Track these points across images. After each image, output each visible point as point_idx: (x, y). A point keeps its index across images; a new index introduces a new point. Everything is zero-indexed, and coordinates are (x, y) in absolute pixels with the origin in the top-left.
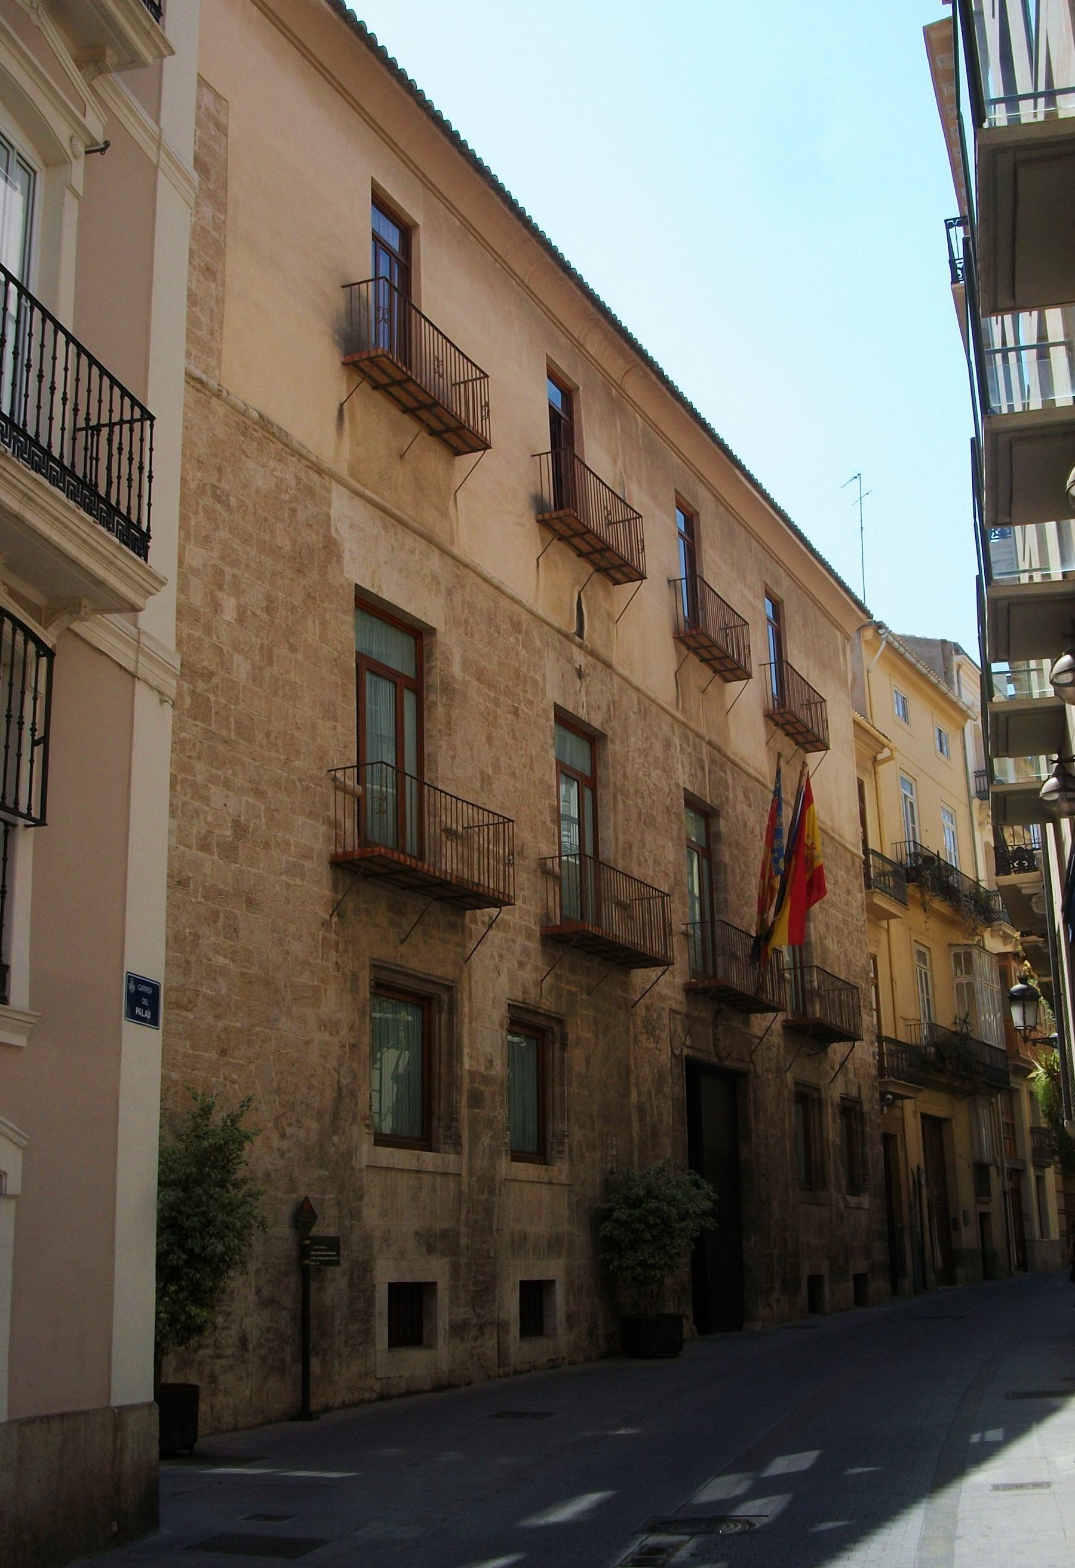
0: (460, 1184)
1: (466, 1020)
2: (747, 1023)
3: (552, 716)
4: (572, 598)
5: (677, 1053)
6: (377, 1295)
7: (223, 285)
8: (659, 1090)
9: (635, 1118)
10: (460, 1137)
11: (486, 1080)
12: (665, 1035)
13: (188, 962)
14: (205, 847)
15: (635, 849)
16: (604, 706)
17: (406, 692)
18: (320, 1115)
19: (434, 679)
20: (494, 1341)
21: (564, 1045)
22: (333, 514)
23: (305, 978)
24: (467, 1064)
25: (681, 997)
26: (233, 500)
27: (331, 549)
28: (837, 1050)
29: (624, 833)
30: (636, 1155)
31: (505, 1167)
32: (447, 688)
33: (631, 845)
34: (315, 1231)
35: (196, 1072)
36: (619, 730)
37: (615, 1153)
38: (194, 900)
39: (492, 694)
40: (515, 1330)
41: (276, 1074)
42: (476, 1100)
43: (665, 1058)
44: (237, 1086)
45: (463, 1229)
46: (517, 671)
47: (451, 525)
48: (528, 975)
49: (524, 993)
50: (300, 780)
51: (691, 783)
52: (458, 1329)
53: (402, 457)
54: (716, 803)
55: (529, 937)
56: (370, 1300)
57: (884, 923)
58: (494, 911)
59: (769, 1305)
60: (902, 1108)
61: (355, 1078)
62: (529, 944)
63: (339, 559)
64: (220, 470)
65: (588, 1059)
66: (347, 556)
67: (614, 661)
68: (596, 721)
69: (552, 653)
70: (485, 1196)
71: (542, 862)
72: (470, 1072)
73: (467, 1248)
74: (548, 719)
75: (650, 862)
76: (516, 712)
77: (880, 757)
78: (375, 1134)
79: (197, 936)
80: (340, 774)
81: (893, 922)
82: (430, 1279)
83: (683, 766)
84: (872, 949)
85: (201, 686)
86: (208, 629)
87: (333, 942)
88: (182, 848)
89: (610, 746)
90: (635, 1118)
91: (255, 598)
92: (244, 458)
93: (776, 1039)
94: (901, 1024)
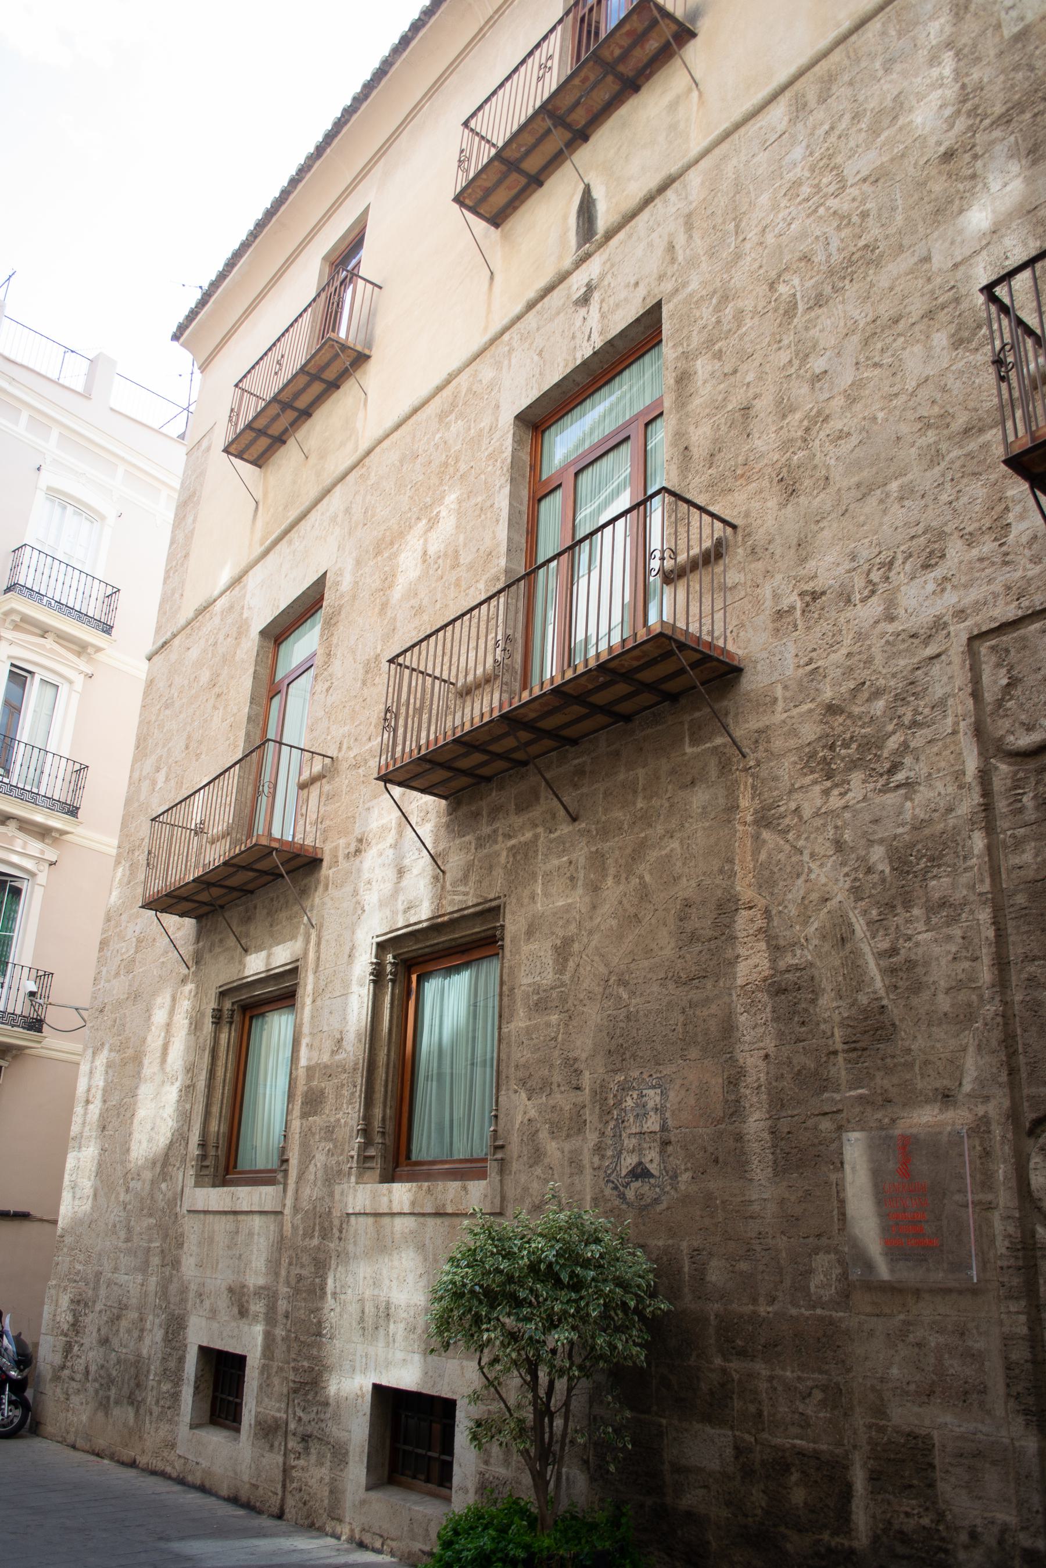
0: (281, 1225)
56: (181, 1360)
70: (316, 1242)
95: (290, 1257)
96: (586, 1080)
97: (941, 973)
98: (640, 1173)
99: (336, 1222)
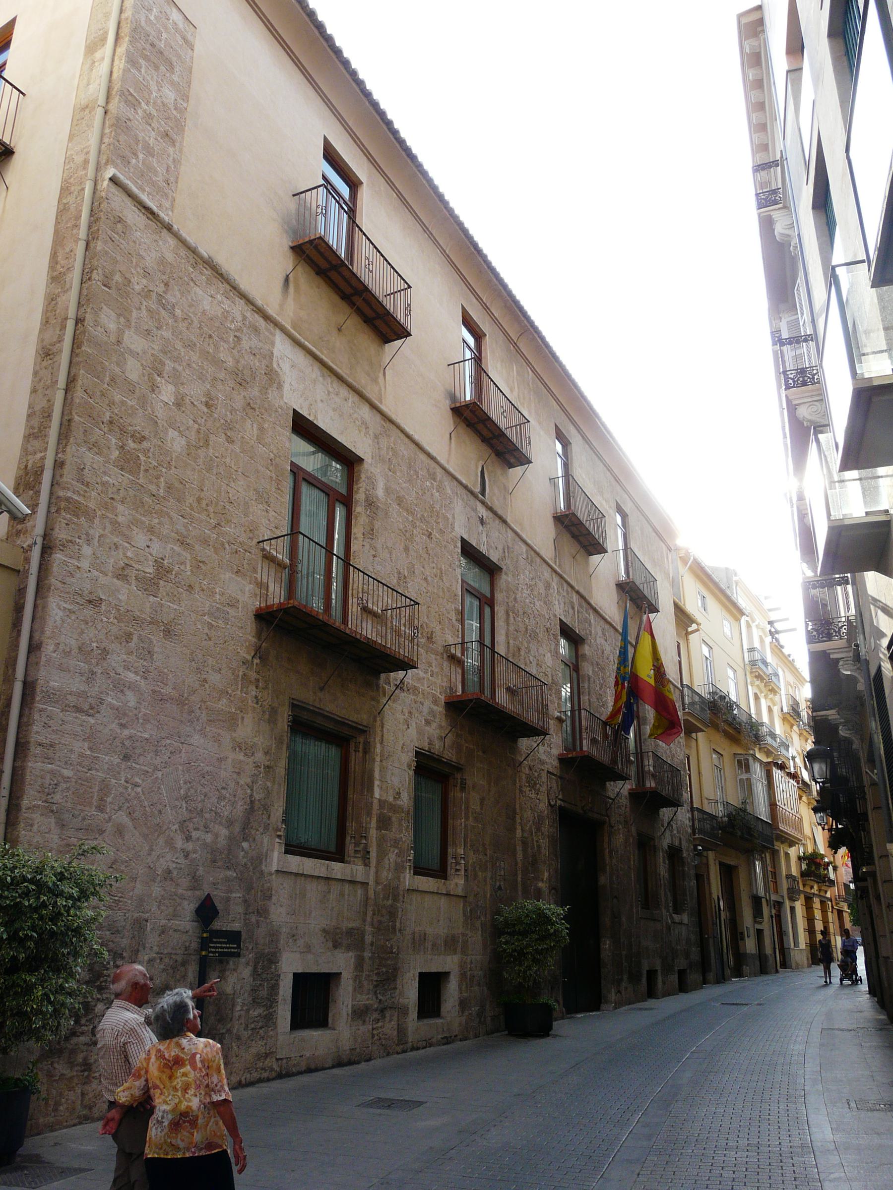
0: (367, 891)
1: (378, 759)
2: (604, 787)
3: (459, 545)
4: (477, 468)
5: (552, 803)
6: (281, 984)
7: (181, 151)
8: (538, 829)
9: (519, 849)
10: (368, 852)
11: (394, 808)
12: (544, 789)
13: (93, 673)
14: (121, 575)
15: (522, 653)
16: (500, 547)
17: (337, 504)
18: (230, 823)
19: (360, 496)
20: (394, 1023)
21: (463, 789)
22: (276, 352)
23: (223, 704)
24: (377, 794)
25: (556, 763)
26: (178, 312)
27: (272, 377)
28: (666, 813)
29: (515, 639)
30: (520, 877)
31: (408, 879)
32: (370, 503)
33: (519, 649)
34: (217, 925)
35: (93, 772)
36: (511, 568)
37: (502, 873)
38: (105, 619)
39: (411, 518)
40: (413, 1014)
41: (185, 783)
42: (384, 823)
43: (543, 806)
44: (139, 790)
45: (368, 929)
46: (432, 507)
47: (380, 390)
48: (433, 731)
49: (429, 744)
50: (229, 542)
51: (565, 616)
52: (359, 1014)
53: (339, 330)
54: (582, 634)
55: (435, 702)
56: (274, 989)
57: (694, 735)
58: (401, 674)
59: (619, 991)
60: (707, 857)
61: (269, 793)
62: (435, 708)
63: (280, 387)
64: (166, 285)
65: (482, 800)
66: (286, 387)
67: (509, 520)
68: (494, 557)
69: (460, 502)
70: (390, 902)
71: (447, 647)
72: (380, 800)
73: (372, 944)
74: (455, 547)
75: (534, 663)
76: (430, 535)
77: (690, 629)
78: (286, 845)
79: (105, 652)
80: (266, 546)
81: (699, 734)
82: (335, 970)
83: (559, 604)
84: (687, 752)
85: (131, 444)
86: (143, 401)
87: (253, 679)
88: (96, 573)
89: (504, 577)
90: (519, 849)
91: (195, 391)
92: (192, 284)
93: (624, 801)
94: (705, 802)
95: (373, 910)
96: (488, 852)
97: (543, 851)
98: (500, 888)
99: (401, 893)
